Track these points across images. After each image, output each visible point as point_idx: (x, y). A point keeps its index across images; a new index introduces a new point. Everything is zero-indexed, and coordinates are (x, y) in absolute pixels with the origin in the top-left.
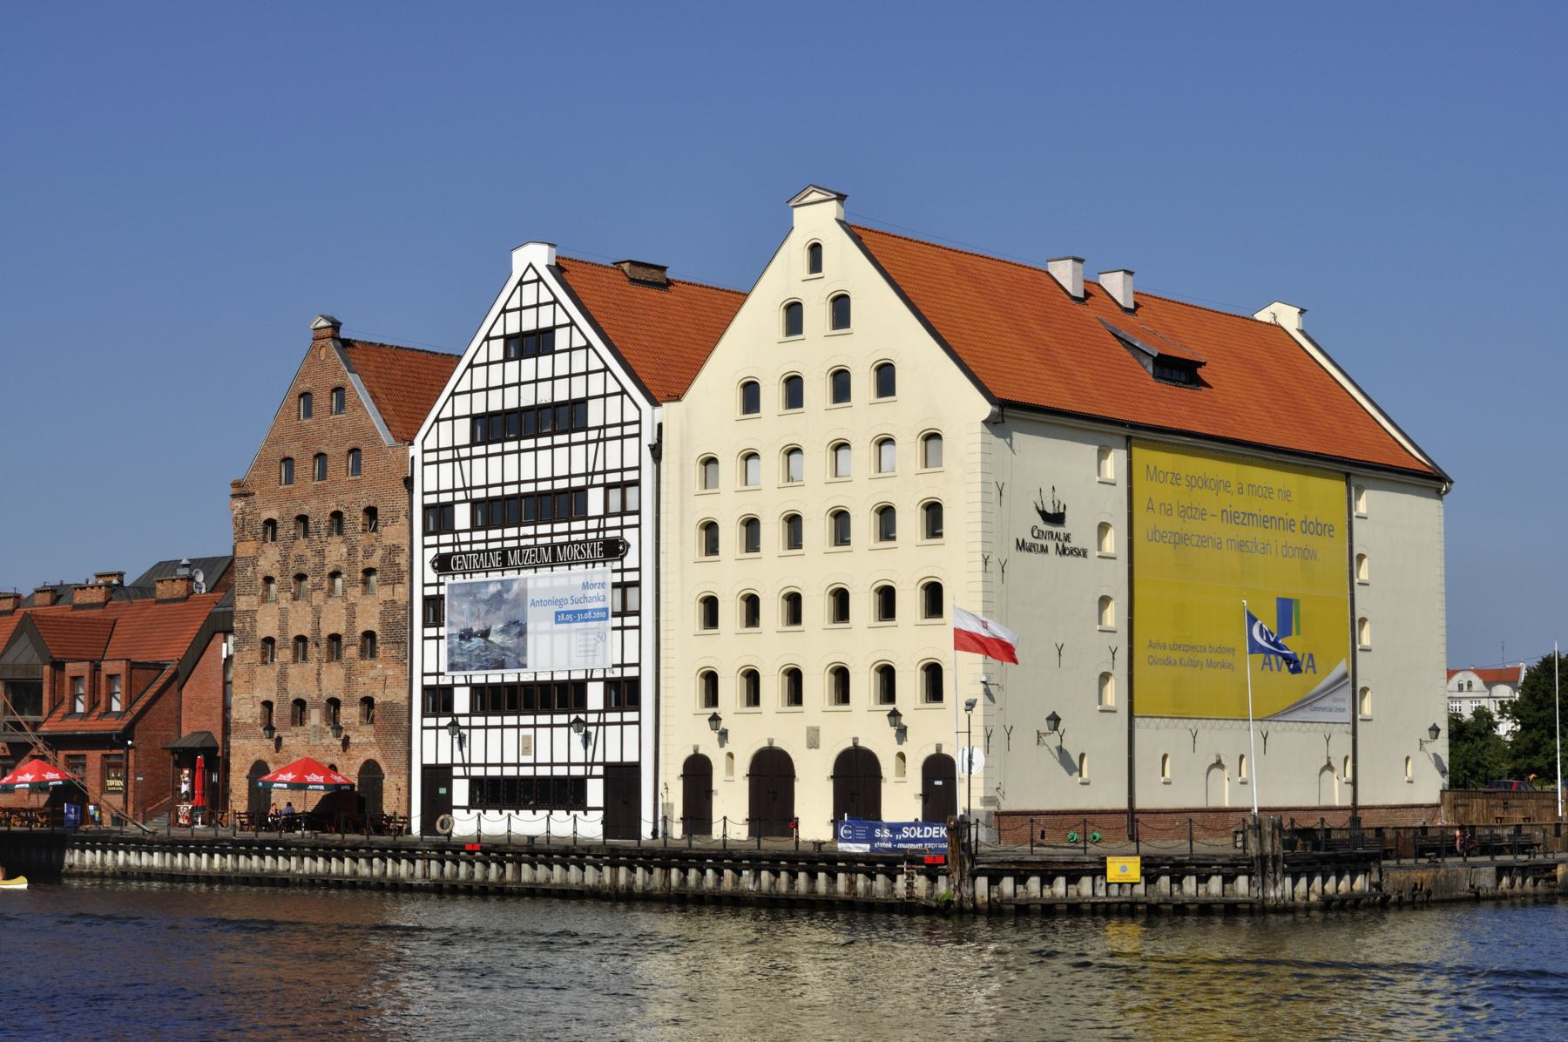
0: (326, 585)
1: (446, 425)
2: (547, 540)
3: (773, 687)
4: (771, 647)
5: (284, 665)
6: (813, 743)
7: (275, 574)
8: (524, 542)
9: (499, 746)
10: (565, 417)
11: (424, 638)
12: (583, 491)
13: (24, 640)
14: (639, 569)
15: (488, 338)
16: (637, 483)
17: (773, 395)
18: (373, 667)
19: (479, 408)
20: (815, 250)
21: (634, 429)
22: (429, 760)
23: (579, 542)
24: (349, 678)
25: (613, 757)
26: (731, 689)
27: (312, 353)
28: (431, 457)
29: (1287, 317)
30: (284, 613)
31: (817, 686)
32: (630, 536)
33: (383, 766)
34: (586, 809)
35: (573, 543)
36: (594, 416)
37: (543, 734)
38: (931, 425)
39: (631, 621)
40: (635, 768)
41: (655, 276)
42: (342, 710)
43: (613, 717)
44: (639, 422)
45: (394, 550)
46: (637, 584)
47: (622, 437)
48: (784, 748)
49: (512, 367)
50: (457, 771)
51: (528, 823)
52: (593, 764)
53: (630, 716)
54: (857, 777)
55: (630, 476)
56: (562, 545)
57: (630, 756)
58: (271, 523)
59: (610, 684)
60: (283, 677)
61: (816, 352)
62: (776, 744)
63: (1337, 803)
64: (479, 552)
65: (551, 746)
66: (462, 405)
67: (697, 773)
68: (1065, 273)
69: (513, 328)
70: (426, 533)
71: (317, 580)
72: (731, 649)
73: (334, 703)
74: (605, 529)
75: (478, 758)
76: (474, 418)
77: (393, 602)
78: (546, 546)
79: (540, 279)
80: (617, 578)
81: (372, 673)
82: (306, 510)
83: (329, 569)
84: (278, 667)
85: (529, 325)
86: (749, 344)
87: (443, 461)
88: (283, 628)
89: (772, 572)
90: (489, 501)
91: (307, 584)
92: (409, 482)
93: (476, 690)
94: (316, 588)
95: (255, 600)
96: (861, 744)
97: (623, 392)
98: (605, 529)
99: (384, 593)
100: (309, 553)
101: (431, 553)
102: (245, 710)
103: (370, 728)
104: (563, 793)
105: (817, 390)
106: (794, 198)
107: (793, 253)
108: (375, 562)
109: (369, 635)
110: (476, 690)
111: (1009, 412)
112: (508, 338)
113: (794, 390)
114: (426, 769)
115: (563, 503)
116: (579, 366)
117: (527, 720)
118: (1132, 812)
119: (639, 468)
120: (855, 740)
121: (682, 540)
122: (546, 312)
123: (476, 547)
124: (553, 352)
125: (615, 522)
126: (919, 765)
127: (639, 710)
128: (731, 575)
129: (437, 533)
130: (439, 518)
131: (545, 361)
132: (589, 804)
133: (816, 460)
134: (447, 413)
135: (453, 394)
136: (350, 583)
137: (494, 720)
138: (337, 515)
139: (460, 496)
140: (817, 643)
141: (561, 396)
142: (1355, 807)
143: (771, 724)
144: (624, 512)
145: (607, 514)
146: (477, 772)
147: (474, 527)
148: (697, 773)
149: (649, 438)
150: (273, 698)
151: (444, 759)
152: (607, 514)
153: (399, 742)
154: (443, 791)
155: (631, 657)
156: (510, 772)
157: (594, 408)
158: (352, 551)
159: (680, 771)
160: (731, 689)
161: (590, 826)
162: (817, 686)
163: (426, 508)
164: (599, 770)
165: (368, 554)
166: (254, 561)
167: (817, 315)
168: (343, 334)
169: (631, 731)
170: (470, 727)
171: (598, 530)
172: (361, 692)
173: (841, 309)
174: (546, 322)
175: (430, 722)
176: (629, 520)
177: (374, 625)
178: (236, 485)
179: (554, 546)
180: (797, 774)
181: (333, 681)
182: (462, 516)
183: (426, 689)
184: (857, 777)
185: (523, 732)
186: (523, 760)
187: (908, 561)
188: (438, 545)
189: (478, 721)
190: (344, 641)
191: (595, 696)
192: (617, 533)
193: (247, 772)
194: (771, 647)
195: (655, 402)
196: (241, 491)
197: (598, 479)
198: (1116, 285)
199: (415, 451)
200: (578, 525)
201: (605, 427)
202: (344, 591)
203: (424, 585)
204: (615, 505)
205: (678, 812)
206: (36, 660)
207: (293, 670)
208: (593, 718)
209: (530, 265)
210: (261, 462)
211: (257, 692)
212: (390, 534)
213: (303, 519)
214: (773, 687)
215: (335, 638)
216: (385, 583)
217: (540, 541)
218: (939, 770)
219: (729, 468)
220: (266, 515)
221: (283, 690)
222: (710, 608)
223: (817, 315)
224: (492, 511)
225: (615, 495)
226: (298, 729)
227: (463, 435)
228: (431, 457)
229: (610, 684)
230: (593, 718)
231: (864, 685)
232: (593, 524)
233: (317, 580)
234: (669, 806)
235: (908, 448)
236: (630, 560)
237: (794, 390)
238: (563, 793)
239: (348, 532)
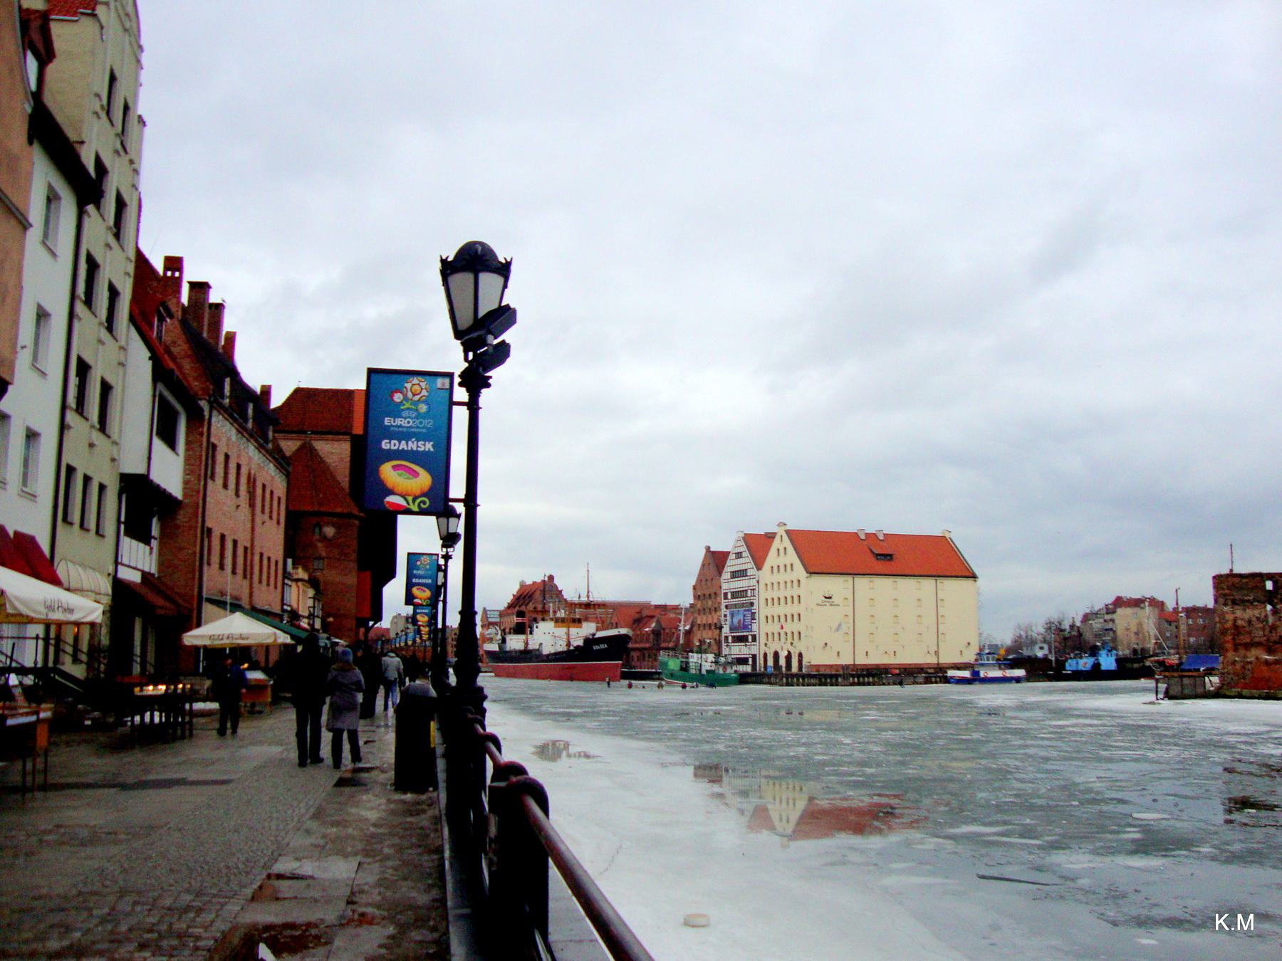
1: (726, 575)
17: (775, 569)
61: (781, 561)
121: (762, 602)
160: (770, 637)
161: (748, 669)
167: (782, 551)
196: (694, 588)
218: (800, 655)
223: (782, 551)
224: (735, 595)
238: (743, 661)
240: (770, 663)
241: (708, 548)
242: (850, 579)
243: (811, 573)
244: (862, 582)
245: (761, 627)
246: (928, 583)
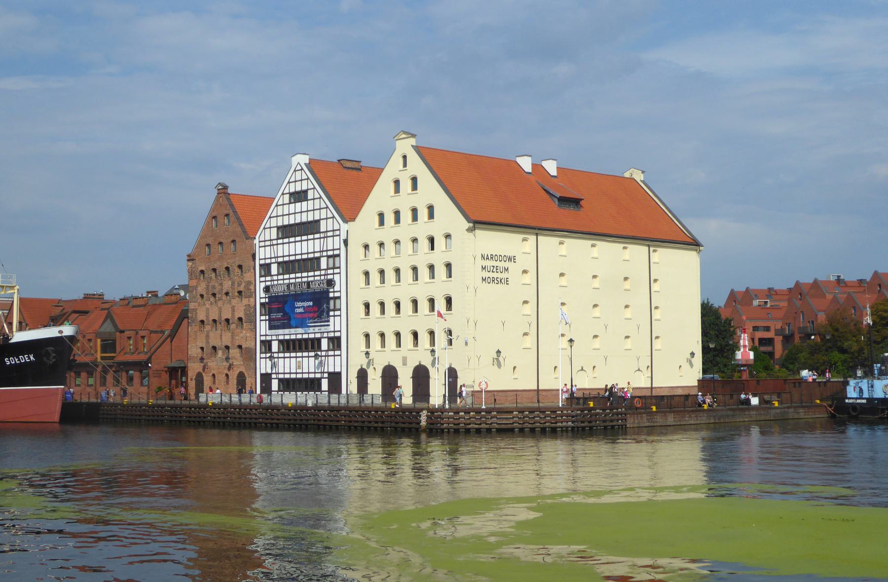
1: (267, 233)
4: (390, 323)
5: (208, 332)
6: (405, 364)
7: (204, 293)
10: (310, 228)
12: (318, 259)
13: (109, 320)
15: (283, 194)
16: (339, 255)
17: (390, 218)
19: (280, 224)
20: (405, 157)
21: (337, 233)
22: (263, 371)
24: (232, 338)
25: (331, 370)
27: (217, 199)
28: (262, 244)
29: (639, 177)
30: (207, 309)
34: (321, 391)
37: (305, 360)
39: (337, 313)
40: (339, 374)
41: (356, 165)
43: (331, 353)
45: (249, 283)
46: (339, 298)
47: (333, 236)
49: (292, 206)
50: (274, 376)
51: (308, 399)
53: (337, 353)
54: (421, 376)
55: (336, 252)
57: (338, 370)
58: (202, 272)
60: (208, 337)
61: (405, 201)
63: (643, 386)
66: (274, 222)
67: (362, 376)
68: (526, 164)
69: (292, 190)
70: (261, 276)
72: (375, 323)
73: (227, 347)
75: (281, 371)
76: (278, 228)
79: (302, 169)
83: (224, 291)
85: (298, 189)
86: (381, 197)
87: (268, 248)
88: (207, 317)
89: (390, 292)
92: (254, 256)
93: (281, 342)
97: (334, 217)
100: (216, 284)
101: (263, 285)
102: (194, 351)
105: (406, 216)
106: (396, 138)
107: (396, 160)
108: (242, 288)
109: (240, 319)
110: (281, 342)
111: (477, 225)
112: (291, 194)
114: (262, 375)
115: (311, 264)
116: (317, 207)
117: (299, 354)
118: (538, 390)
122: (304, 182)
124: (307, 200)
128: (374, 294)
129: (265, 276)
130: (266, 268)
131: (304, 203)
133: (407, 246)
134: (268, 225)
135: (270, 217)
137: (287, 355)
138: (227, 269)
139: (273, 260)
140: (406, 322)
142: (652, 388)
144: (334, 268)
145: (328, 269)
146: (281, 376)
148: (362, 376)
149: (343, 237)
150: (204, 346)
151: (269, 371)
152: (328, 269)
153: (252, 364)
155: (337, 328)
156: (293, 376)
157: (323, 223)
160: (375, 340)
161: (323, 397)
163: (261, 265)
164: (326, 375)
165: (239, 285)
168: (229, 191)
169: (338, 359)
170: (278, 358)
172: (238, 343)
174: (304, 188)
175: (263, 355)
177: (242, 315)
178: (189, 256)
181: (226, 339)
182: (274, 269)
183: (262, 342)
184: (421, 376)
185: (298, 359)
187: (439, 288)
189: (281, 355)
191: (324, 344)
194: (390, 323)
195: (346, 221)
196: (191, 259)
197: (324, 254)
198: (551, 167)
199: (256, 241)
200: (317, 273)
204: (331, 265)
206: (113, 330)
207: (211, 334)
208: (324, 353)
210: (198, 246)
212: (248, 276)
213: (214, 270)
215: (227, 320)
218: (452, 374)
219: (374, 249)
221: (208, 342)
225: (331, 260)
228: (262, 244)
229: (331, 339)
230: (324, 353)
231: (424, 338)
232: (323, 272)
236: (337, 288)
238: (312, 385)
239: (232, 276)
240: (375, 387)
241: (223, 190)
242: (532, 238)
243: (477, 223)
244: (548, 242)
245: (349, 321)
246: (638, 251)
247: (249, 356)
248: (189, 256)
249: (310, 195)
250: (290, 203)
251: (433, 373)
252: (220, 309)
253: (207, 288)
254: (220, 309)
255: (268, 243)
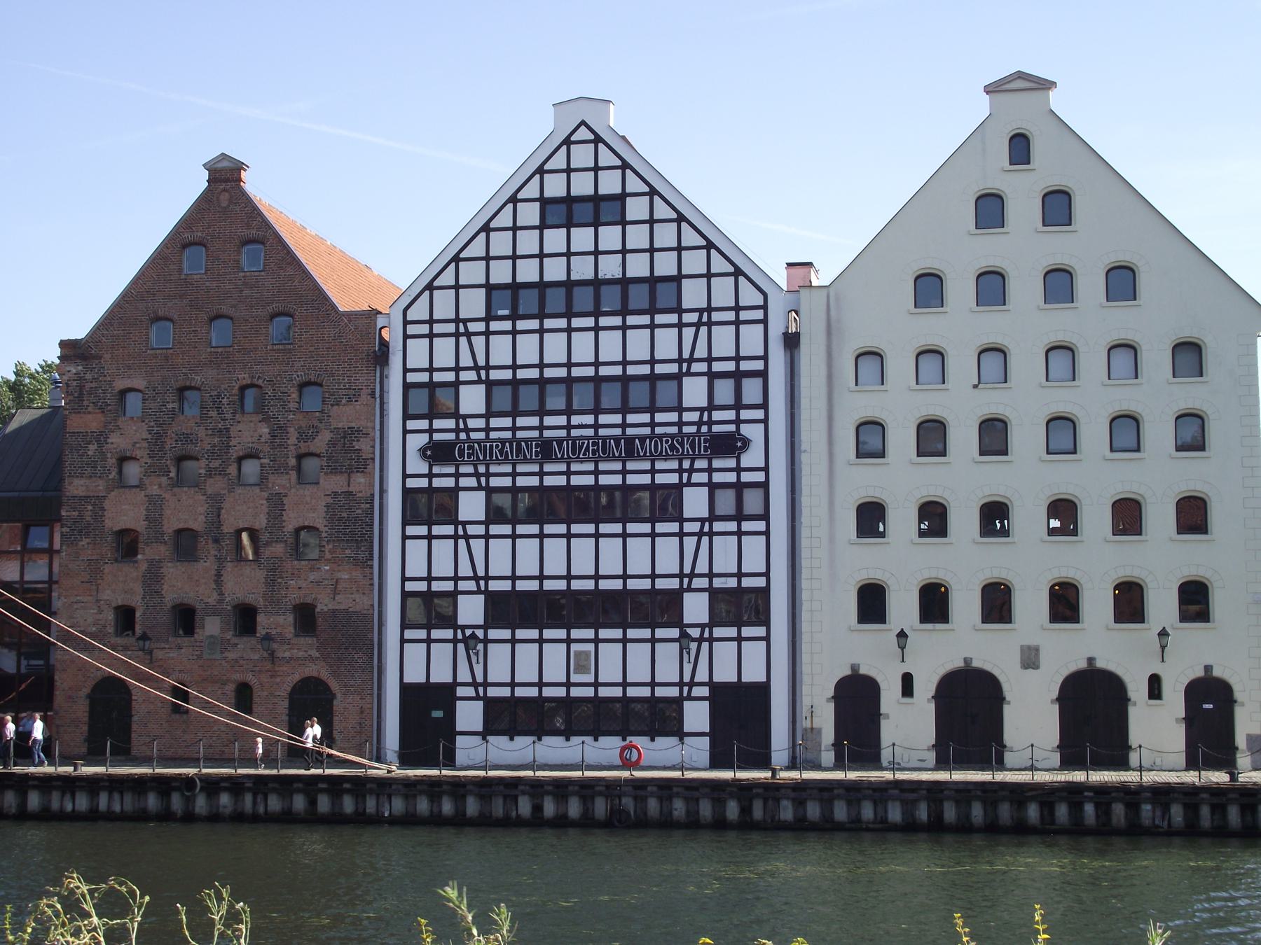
0: (232, 470)
2: (618, 431)
3: (965, 604)
4: (965, 562)
8: (574, 433)
9: (535, 663)
11: (405, 537)
14: (766, 469)
17: (960, 290)
18: (312, 569)
21: (759, 315)
22: (415, 675)
23: (672, 436)
24: (271, 581)
25: (725, 674)
26: (903, 606)
31: (1031, 604)
32: (753, 432)
33: (334, 685)
34: (681, 734)
35: (661, 437)
36: (693, 294)
38: (1187, 333)
40: (762, 691)
42: (261, 618)
44: (764, 307)
45: (351, 434)
46: (765, 486)
48: (988, 667)
50: (461, 691)
52: (692, 684)
56: (642, 439)
57: (753, 674)
59: (715, 595)
60: (153, 578)
62: (976, 664)
64: (503, 441)
65: (628, 663)
66: (472, 273)
69: (555, 187)
70: (407, 416)
71: (216, 464)
72: (903, 562)
74: (710, 423)
76: (490, 288)
77: (349, 493)
78: (617, 440)
79: (598, 140)
80: (731, 477)
81: (313, 576)
82: (197, 379)
83: (235, 453)
84: (144, 566)
88: (154, 519)
90: (515, 383)
91: (195, 468)
92: (381, 356)
94: (211, 473)
95: (101, 485)
96: (1100, 664)
98: (710, 423)
99: (336, 483)
103: (309, 640)
104: (660, 717)
112: (544, 202)
113: (992, 286)
114: (407, 690)
119: (765, 358)
120: (1091, 660)
123: (493, 435)
124: (624, 223)
125: (731, 415)
126: (1182, 688)
127: (766, 623)
130: (431, 398)
132: (687, 728)
136: (278, 468)
141: (638, 267)
143: (965, 641)
145: (711, 407)
147: (488, 415)
150: (136, 600)
151: (441, 675)
152: (711, 407)
154: (438, 714)
158: (278, 432)
159: (831, 693)
162: (1031, 604)
163: (407, 387)
164: (704, 691)
166: (101, 438)
167: (1023, 206)
170: (486, 641)
171: (699, 424)
172: (294, 597)
173: (1057, 207)
176: (745, 414)
177: (317, 518)
179: (630, 441)
180: (1008, 694)
181: (244, 584)
182: (472, 399)
185: (574, 647)
186: (575, 678)
188: (431, 431)
190: (264, 537)
191: (696, 608)
192: (732, 428)
193: (87, 690)
197: (702, 367)
200: (673, 417)
201: (710, 309)
202: (262, 482)
203: (405, 476)
205: (828, 736)
209: (583, 123)
211: (106, 595)
212: (344, 416)
214: (965, 604)
216: (334, 468)
217: (602, 432)
220: (121, 384)
222: (871, 518)
223: (1023, 206)
226: (186, 641)
227: (474, 304)
231: (1097, 603)
232: (688, 417)
233: (216, 464)
234: (814, 732)
235: (1157, 359)
236: (753, 457)
237: (992, 286)
238: (660, 717)
247: (356, 637)
248: (64, 344)
249: (636, 208)
250: (542, 227)
251: (1137, 690)
252: (216, 504)
253: (156, 441)
254: (216, 504)
255: (451, 328)
